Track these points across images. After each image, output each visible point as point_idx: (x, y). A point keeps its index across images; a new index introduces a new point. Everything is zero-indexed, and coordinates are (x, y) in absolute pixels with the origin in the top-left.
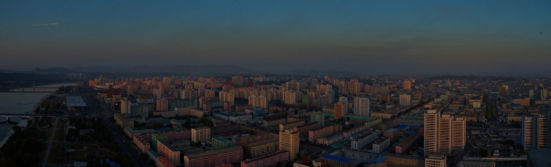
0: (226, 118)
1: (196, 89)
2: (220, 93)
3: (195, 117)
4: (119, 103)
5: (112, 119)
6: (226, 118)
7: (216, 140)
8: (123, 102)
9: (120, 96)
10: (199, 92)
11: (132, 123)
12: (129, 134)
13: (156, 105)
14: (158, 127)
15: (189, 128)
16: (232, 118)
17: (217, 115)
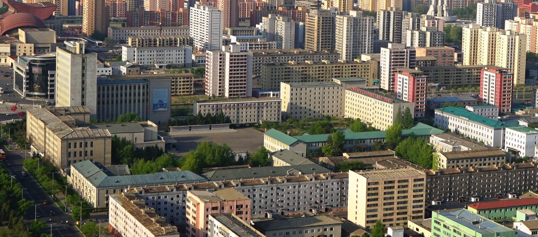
0: (485, 134)
1: (366, 13)
2: (467, 33)
3: (364, 127)
4: (51, 64)
5: (18, 128)
6: (485, 134)
7: (449, 222)
8: (64, 61)
9: (51, 36)
10: (380, 25)
11: (103, 149)
12: (90, 193)
13: (202, 72)
14: (215, 163)
15: (339, 170)
16: (516, 139)
17: (455, 122)
